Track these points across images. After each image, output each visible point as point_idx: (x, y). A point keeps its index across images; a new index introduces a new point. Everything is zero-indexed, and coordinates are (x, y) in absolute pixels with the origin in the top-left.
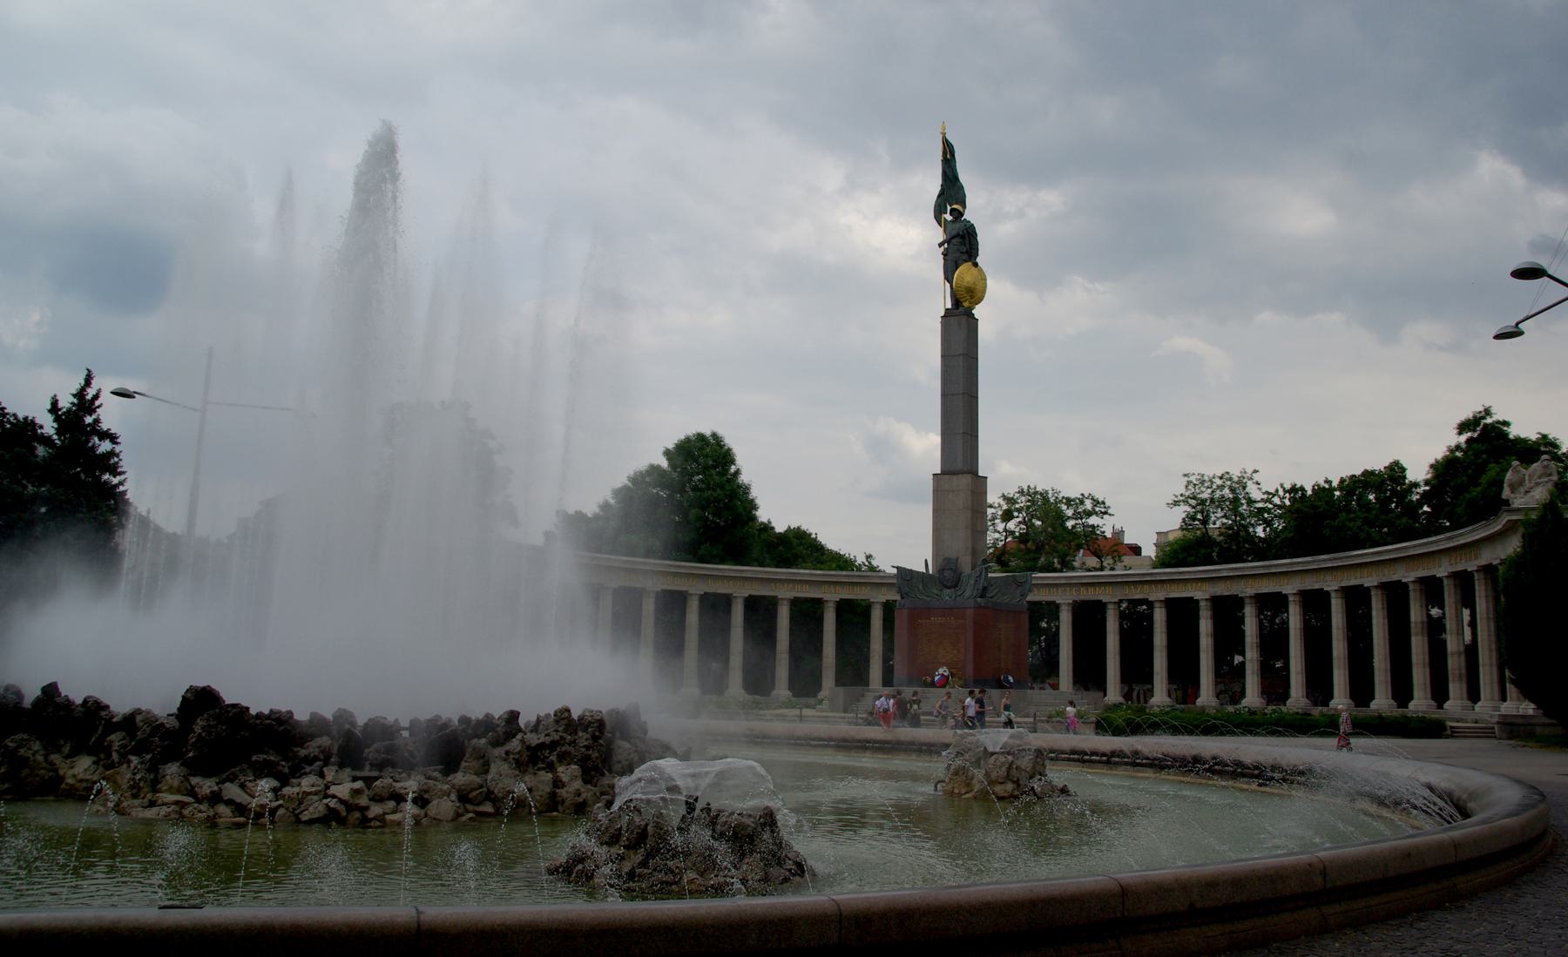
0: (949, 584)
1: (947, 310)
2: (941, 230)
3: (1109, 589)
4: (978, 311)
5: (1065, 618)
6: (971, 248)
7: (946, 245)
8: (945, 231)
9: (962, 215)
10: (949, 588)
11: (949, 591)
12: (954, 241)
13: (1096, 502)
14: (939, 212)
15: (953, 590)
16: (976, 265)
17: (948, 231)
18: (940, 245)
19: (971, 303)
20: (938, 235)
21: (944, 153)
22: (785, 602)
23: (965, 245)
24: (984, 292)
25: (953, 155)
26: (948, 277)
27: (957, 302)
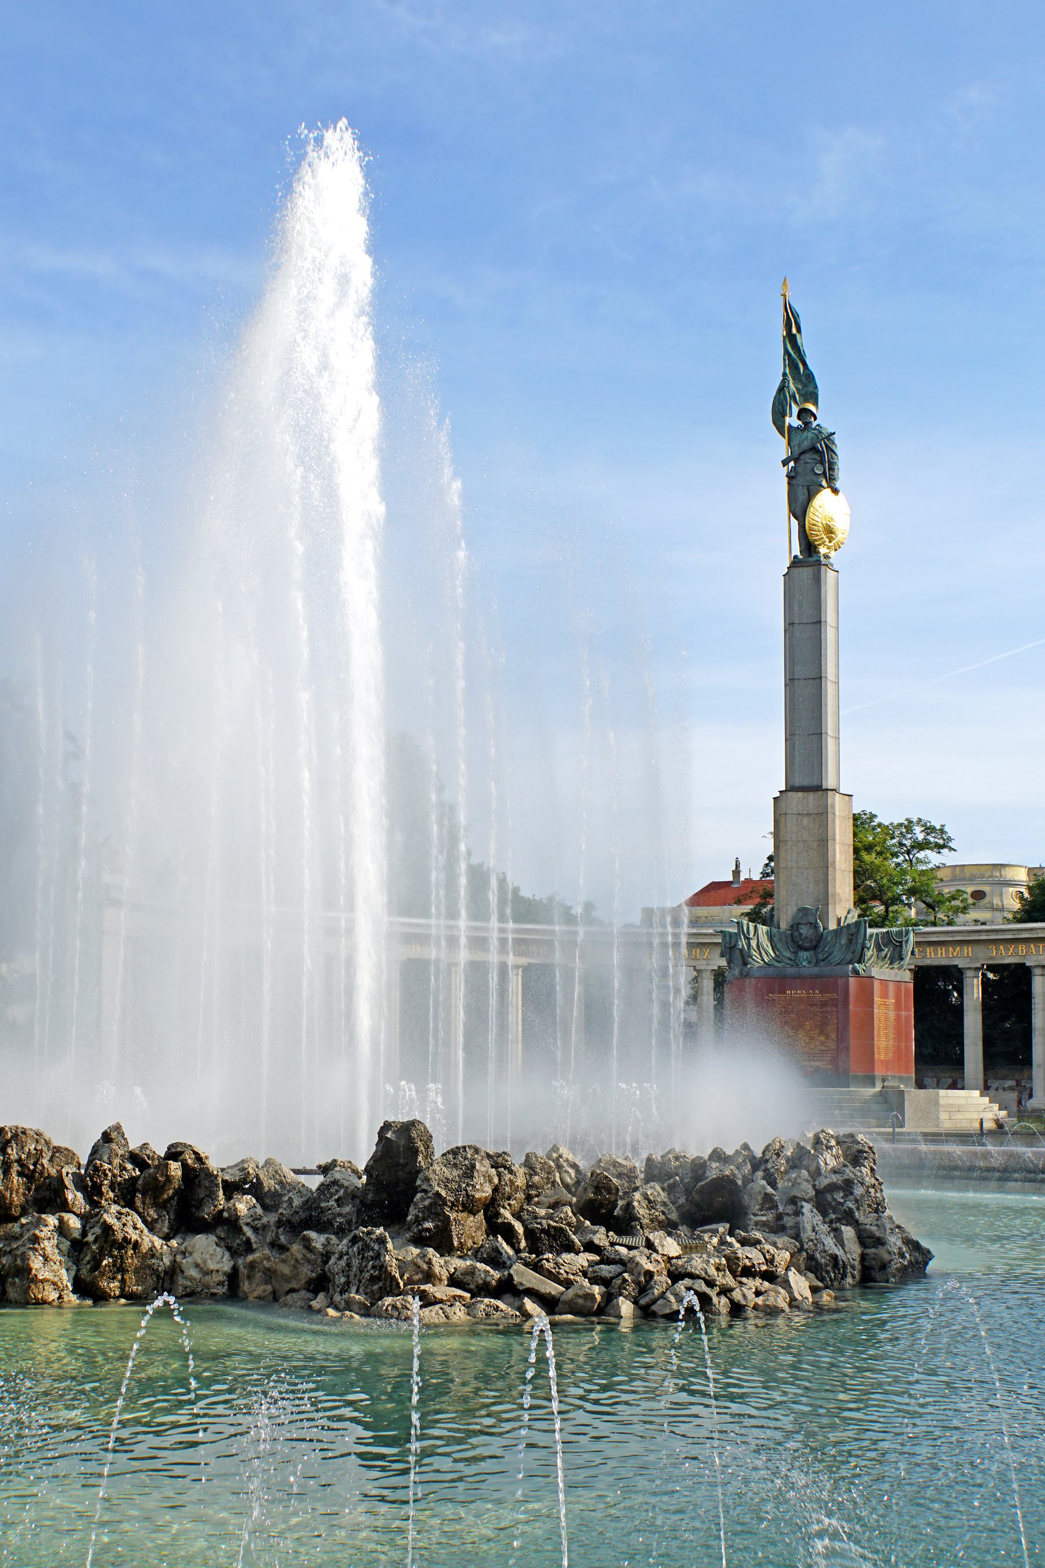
0: (807, 945)
2: (784, 442)
3: (968, 950)
5: (974, 992)
6: (829, 469)
7: (792, 464)
8: (789, 444)
10: (806, 949)
12: (808, 457)
13: (929, 829)
14: (779, 414)
17: (795, 442)
18: (785, 463)
19: (829, 548)
23: (822, 462)
25: (799, 330)
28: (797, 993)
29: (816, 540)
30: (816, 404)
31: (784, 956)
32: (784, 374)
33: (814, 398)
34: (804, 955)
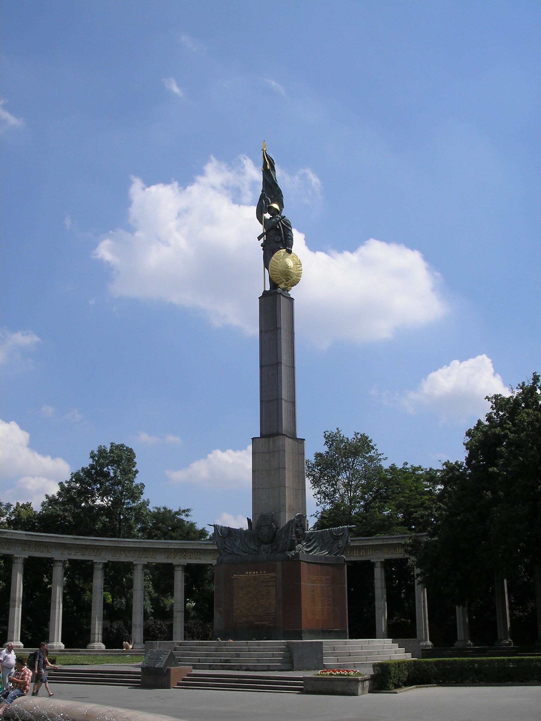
4: (293, 292)
8: (265, 227)
9: (278, 212)
10: (266, 544)
11: (266, 546)
12: (272, 232)
15: (269, 545)
16: (290, 252)
18: (259, 238)
19: (286, 285)
20: (260, 229)
21: (265, 164)
22: (180, 568)
24: (299, 275)
26: (266, 265)
27: (274, 285)
29: (277, 280)
30: (281, 205)
31: (251, 549)
32: (262, 191)
33: (280, 201)
34: (264, 547)
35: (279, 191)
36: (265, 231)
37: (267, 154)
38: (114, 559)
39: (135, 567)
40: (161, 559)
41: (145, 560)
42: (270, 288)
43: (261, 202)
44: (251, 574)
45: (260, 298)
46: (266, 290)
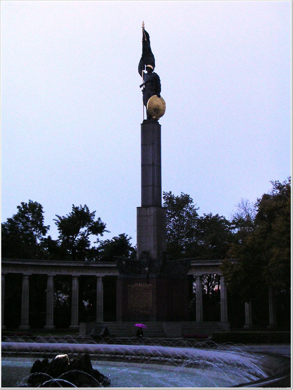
1: (144, 120)
4: (161, 121)
8: (144, 79)
9: (153, 70)
12: (148, 83)
16: (159, 96)
17: (145, 79)
18: (141, 86)
19: (156, 116)
20: (140, 80)
22: (76, 278)
24: (164, 111)
26: (145, 104)
28: (138, 285)
29: (152, 114)
32: (142, 55)
35: (153, 56)
36: (144, 82)
37: (145, 30)
38: (35, 272)
39: (49, 278)
40: (64, 273)
41: (54, 273)
42: (147, 118)
43: (141, 63)
44: (138, 285)
45: (142, 125)
46: (144, 119)
